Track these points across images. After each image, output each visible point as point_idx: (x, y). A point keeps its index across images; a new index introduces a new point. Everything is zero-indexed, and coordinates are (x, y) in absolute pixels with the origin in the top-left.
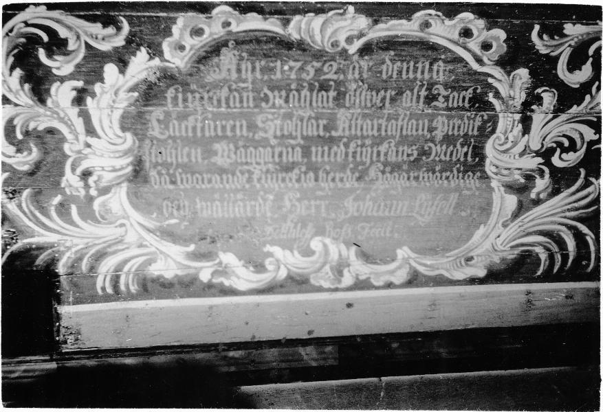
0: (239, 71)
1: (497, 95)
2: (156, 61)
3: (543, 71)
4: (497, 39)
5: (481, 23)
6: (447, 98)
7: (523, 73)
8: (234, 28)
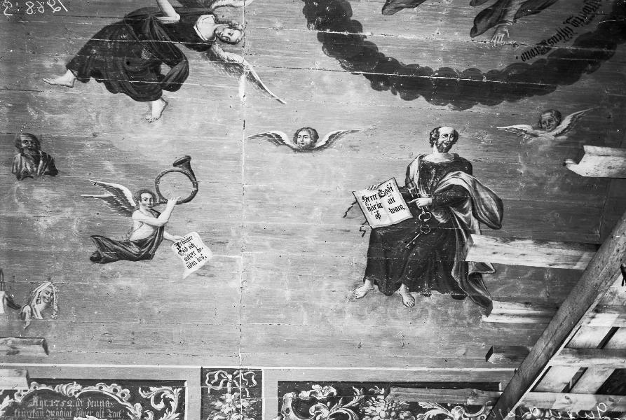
0: (39, 403)
1: (130, 413)
2: (12, 400)
3: (146, 404)
4: (127, 393)
5: (120, 387)
6: (112, 414)
7: (138, 405)
8: (37, 389)
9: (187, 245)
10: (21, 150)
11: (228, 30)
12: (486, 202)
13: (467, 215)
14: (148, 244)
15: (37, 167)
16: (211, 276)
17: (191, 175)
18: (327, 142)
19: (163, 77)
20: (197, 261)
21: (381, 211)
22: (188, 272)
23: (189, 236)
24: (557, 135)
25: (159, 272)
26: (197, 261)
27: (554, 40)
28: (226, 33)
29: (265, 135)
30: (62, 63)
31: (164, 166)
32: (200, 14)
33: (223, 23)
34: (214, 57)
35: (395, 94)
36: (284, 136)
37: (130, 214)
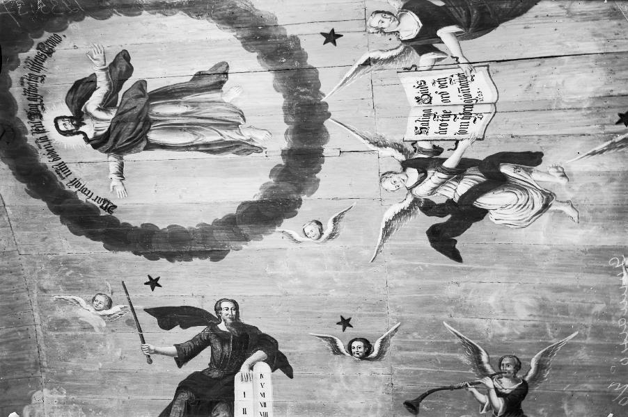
11: (384, 25)
28: (388, 24)
32: (418, 38)
33: (391, 33)
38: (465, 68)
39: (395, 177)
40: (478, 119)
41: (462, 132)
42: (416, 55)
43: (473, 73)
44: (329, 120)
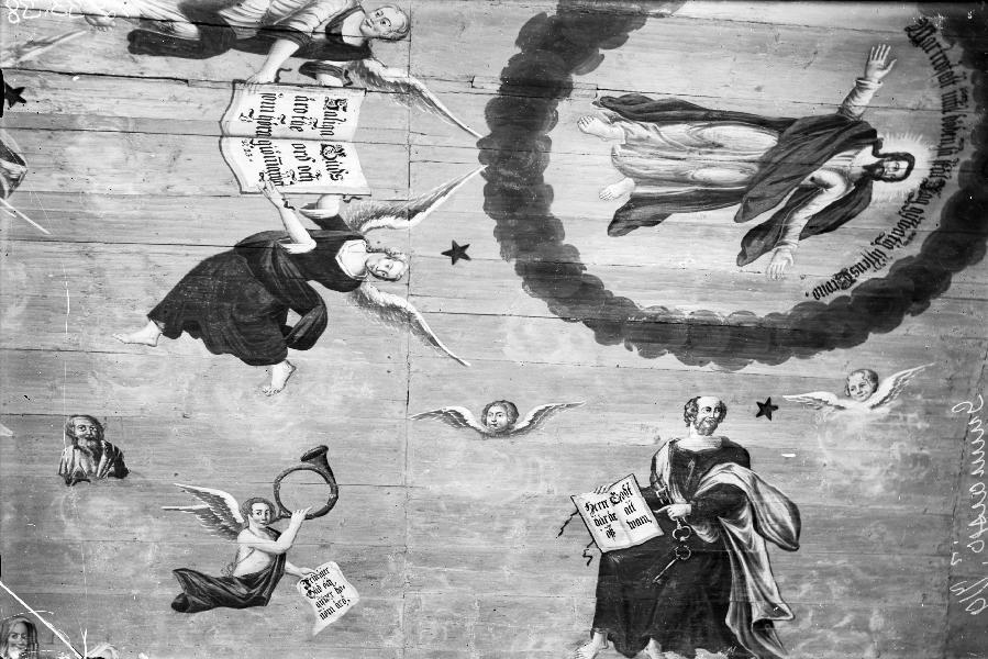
9: (320, 582)
10: (75, 440)
11: (387, 262)
12: (774, 508)
13: (745, 530)
14: (259, 583)
15: (97, 465)
16: (357, 630)
17: (328, 474)
18: (531, 422)
19: (290, 328)
20: (335, 608)
21: (615, 526)
22: (322, 624)
23: (323, 567)
24: (873, 407)
25: (276, 625)
26: (335, 608)
27: (860, 268)
28: (380, 263)
29: (440, 412)
30: (143, 312)
31: (286, 462)
32: (342, 240)
33: (377, 251)
34: (364, 302)
35: (630, 349)
36: (467, 414)
37: (234, 534)
38: (276, 193)
39: (383, 30)
40: (247, 114)
41: (270, 97)
42: (344, 217)
43: (262, 184)
44: (481, 137)
